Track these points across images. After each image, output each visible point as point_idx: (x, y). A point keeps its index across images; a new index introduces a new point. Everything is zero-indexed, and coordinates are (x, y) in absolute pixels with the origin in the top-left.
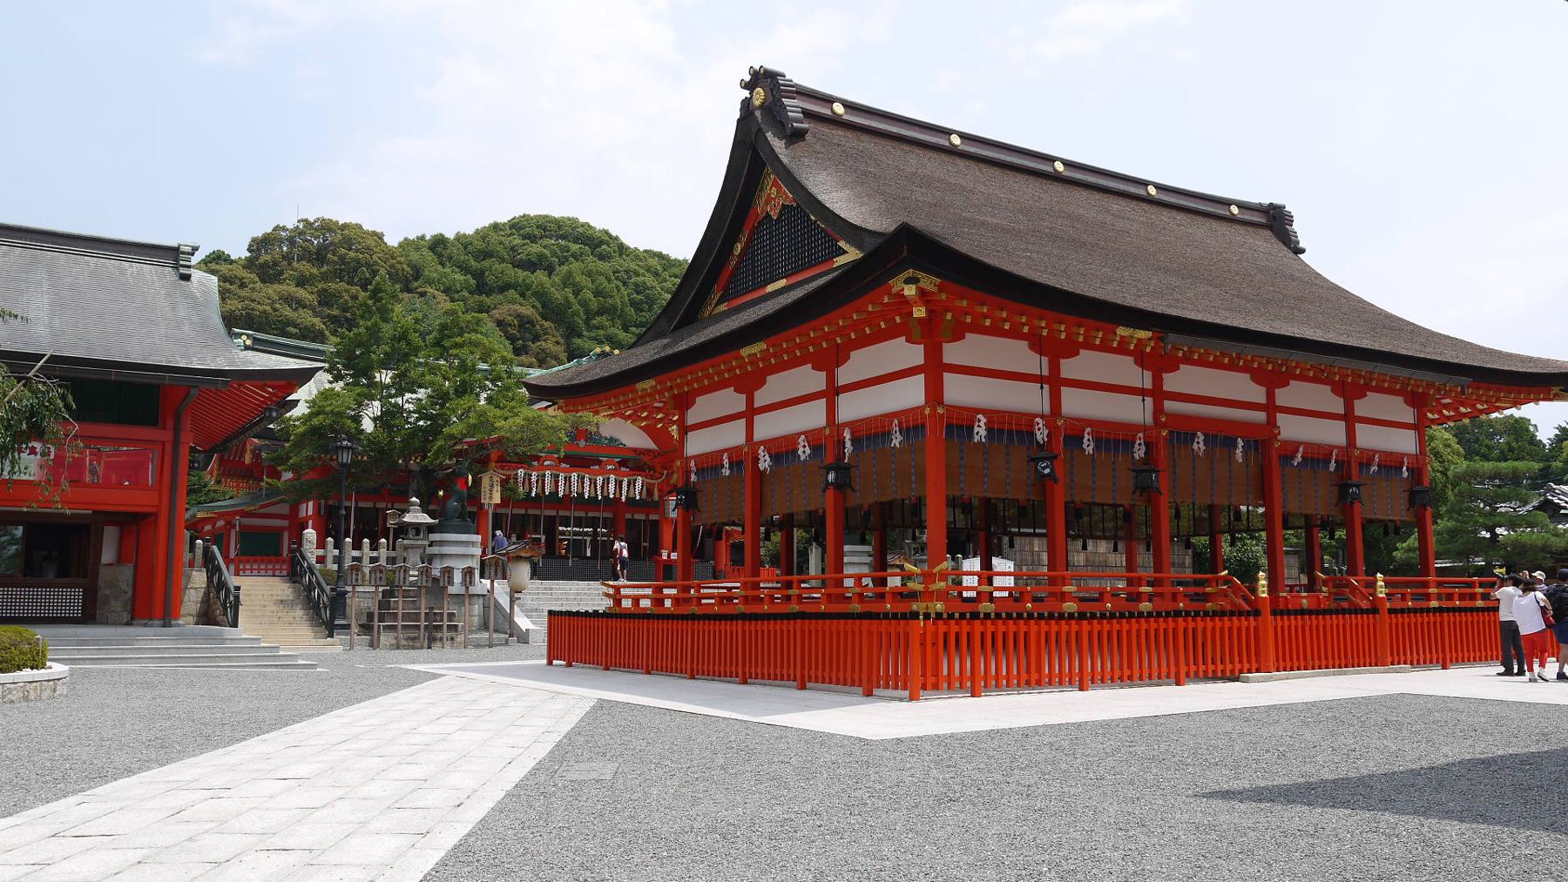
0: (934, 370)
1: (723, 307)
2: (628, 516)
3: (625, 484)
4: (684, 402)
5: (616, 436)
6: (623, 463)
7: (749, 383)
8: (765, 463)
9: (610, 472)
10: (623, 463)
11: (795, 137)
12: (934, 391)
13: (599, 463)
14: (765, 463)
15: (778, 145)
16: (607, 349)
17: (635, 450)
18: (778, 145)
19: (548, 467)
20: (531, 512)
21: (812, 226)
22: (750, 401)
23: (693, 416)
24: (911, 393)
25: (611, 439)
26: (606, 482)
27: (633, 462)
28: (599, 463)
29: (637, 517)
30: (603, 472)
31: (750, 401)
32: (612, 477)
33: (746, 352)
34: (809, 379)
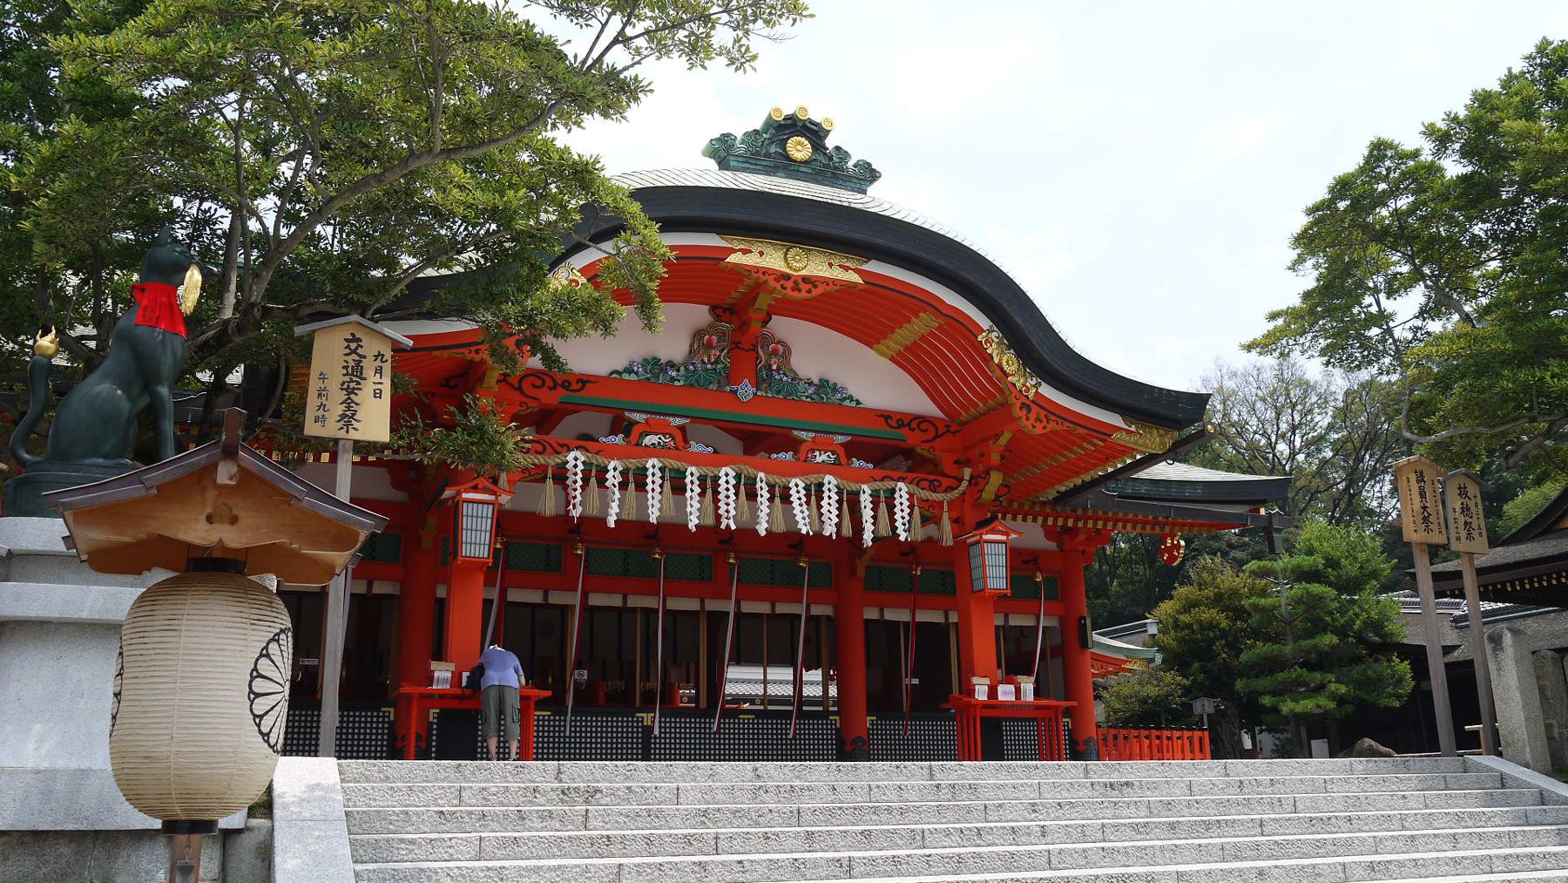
2: (871, 614)
3: (865, 499)
5: (837, 376)
6: (854, 449)
9: (824, 468)
10: (854, 449)
13: (794, 445)
17: (886, 416)
19: (653, 451)
20: (635, 601)
25: (824, 385)
26: (815, 493)
27: (883, 447)
28: (794, 445)
29: (891, 615)
30: (804, 467)
32: (830, 481)
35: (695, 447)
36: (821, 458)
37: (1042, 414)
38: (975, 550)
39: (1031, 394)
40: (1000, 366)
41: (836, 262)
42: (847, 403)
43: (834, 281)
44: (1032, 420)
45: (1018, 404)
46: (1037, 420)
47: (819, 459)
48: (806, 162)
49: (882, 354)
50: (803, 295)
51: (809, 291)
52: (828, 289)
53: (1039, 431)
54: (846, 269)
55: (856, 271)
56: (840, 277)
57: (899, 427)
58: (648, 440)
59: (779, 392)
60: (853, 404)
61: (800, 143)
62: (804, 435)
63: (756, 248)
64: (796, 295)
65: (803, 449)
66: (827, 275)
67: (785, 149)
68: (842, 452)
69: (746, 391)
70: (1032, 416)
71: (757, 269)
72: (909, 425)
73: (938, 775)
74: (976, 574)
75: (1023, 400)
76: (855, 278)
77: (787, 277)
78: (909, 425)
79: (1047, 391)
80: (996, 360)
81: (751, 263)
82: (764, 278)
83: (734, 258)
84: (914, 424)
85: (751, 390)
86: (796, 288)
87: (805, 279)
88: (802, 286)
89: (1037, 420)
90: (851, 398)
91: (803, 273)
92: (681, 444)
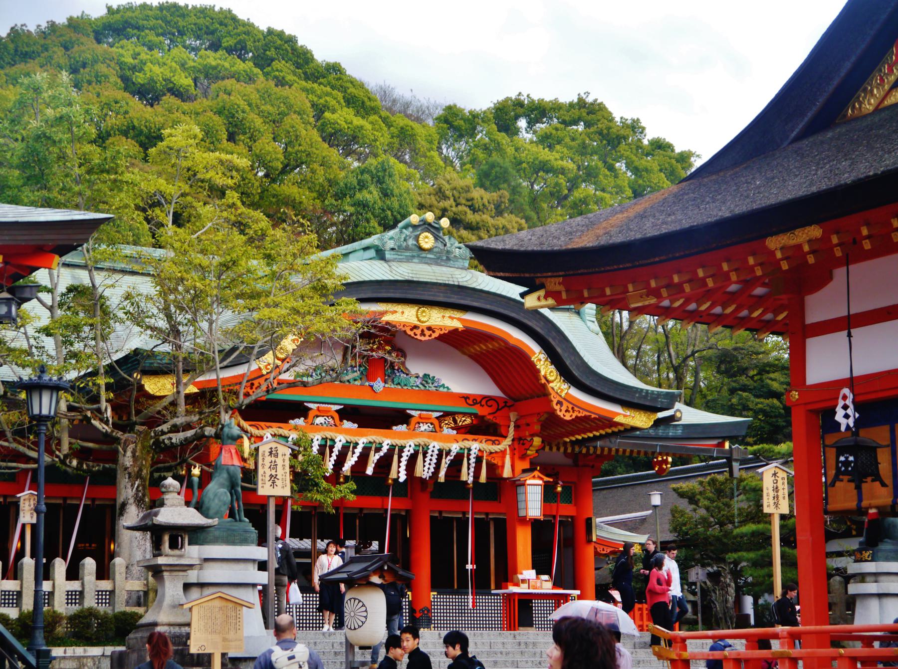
16: (430, 216)
17: (466, 398)
35: (347, 424)
36: (424, 427)
37: (570, 406)
38: (520, 490)
39: (563, 395)
40: (545, 378)
41: (449, 313)
42: (441, 389)
43: (445, 327)
44: (563, 412)
45: (555, 402)
46: (567, 411)
47: (422, 429)
48: (429, 250)
49: (464, 353)
50: (427, 338)
51: (430, 336)
52: (442, 333)
53: (568, 418)
54: (452, 318)
55: (459, 319)
56: (449, 324)
57: (474, 404)
58: (319, 420)
59: (399, 384)
60: (445, 390)
61: (426, 237)
62: (413, 413)
63: (399, 308)
64: (423, 338)
65: (413, 421)
66: (441, 324)
67: (417, 241)
68: (436, 422)
69: (379, 385)
70: (564, 408)
71: (400, 323)
72: (480, 402)
73: (517, 637)
74: (521, 505)
75: (558, 398)
76: (459, 325)
77: (415, 327)
78: (480, 402)
79: (575, 393)
80: (543, 373)
81: (396, 320)
82: (403, 329)
83: (387, 318)
84: (483, 402)
85: (382, 384)
86: (423, 334)
87: (429, 328)
88: (427, 333)
89: (567, 411)
90: (443, 385)
91: (427, 324)
92: (338, 422)
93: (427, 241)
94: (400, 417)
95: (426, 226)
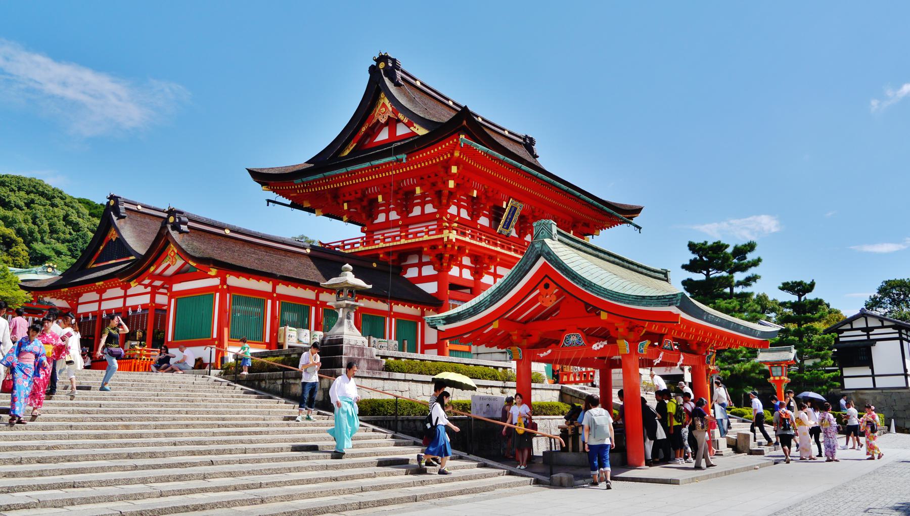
0: (153, 294)
1: (95, 266)
4: (80, 295)
7: (101, 291)
8: (104, 316)
11: (120, 217)
12: (153, 299)
14: (104, 316)
15: (115, 218)
18: (115, 218)
21: (121, 248)
22: (101, 297)
23: (81, 300)
24: (146, 299)
31: (101, 297)
33: (97, 284)
34: (119, 292)
93: (50, 270)
94: (41, 312)
95: (49, 267)
